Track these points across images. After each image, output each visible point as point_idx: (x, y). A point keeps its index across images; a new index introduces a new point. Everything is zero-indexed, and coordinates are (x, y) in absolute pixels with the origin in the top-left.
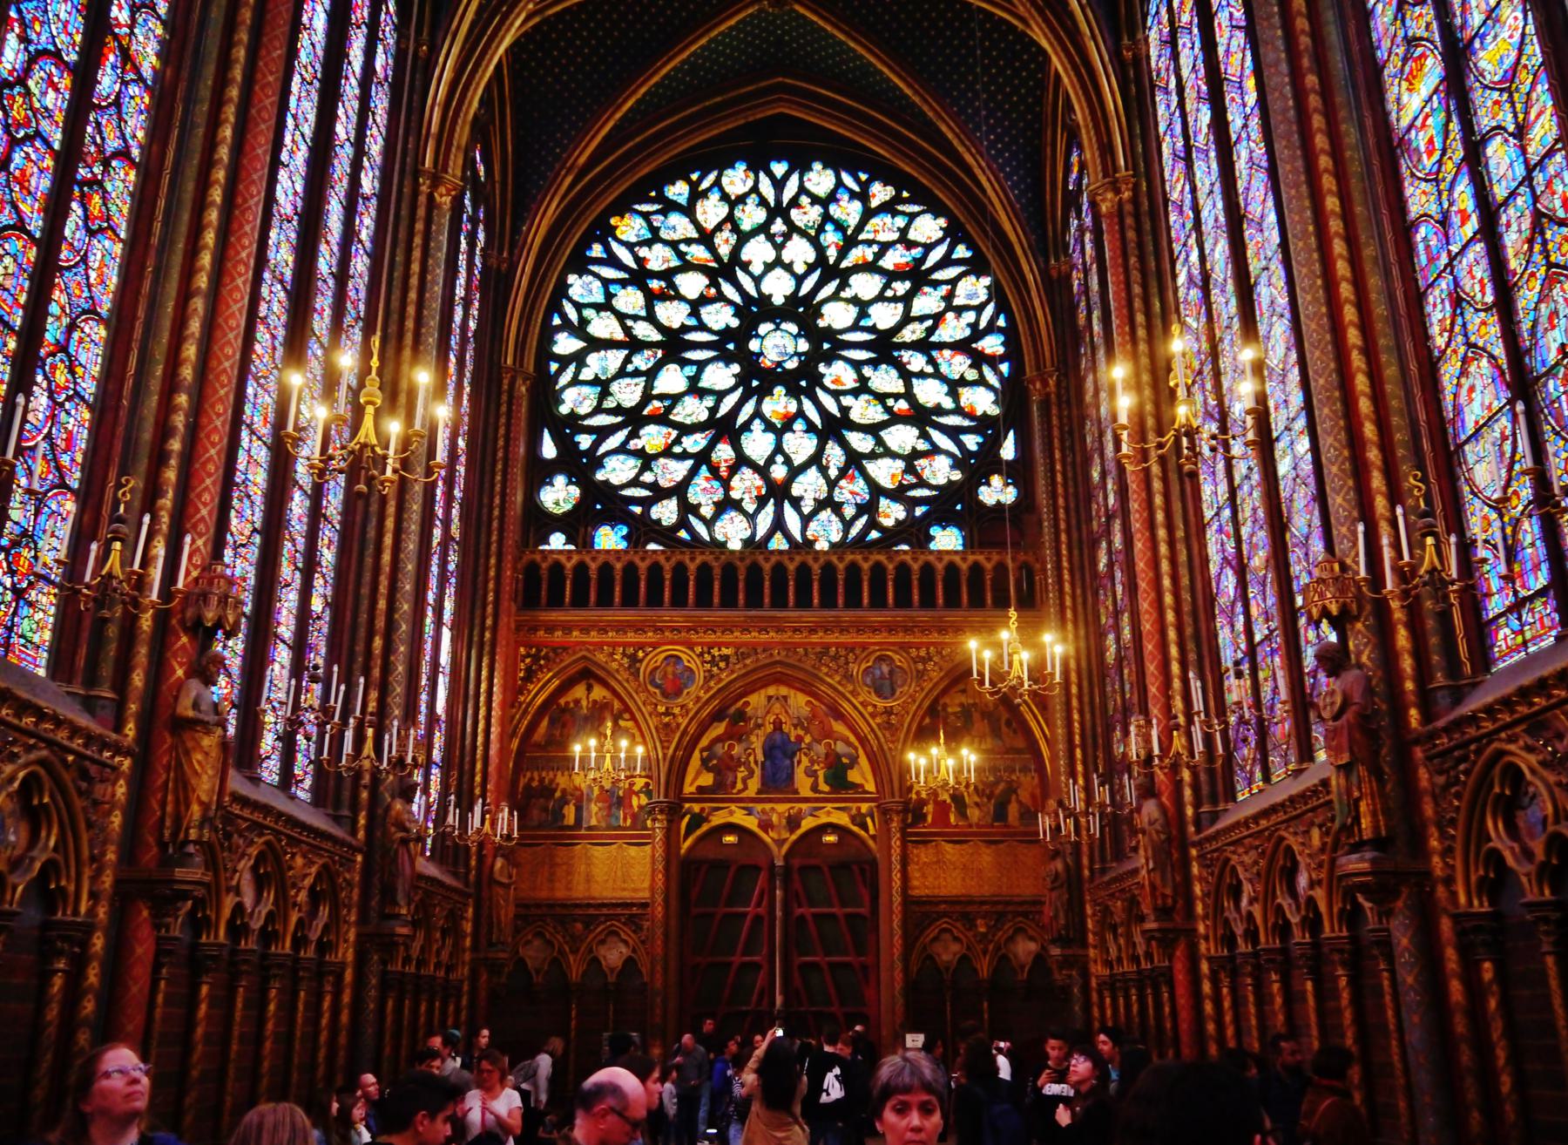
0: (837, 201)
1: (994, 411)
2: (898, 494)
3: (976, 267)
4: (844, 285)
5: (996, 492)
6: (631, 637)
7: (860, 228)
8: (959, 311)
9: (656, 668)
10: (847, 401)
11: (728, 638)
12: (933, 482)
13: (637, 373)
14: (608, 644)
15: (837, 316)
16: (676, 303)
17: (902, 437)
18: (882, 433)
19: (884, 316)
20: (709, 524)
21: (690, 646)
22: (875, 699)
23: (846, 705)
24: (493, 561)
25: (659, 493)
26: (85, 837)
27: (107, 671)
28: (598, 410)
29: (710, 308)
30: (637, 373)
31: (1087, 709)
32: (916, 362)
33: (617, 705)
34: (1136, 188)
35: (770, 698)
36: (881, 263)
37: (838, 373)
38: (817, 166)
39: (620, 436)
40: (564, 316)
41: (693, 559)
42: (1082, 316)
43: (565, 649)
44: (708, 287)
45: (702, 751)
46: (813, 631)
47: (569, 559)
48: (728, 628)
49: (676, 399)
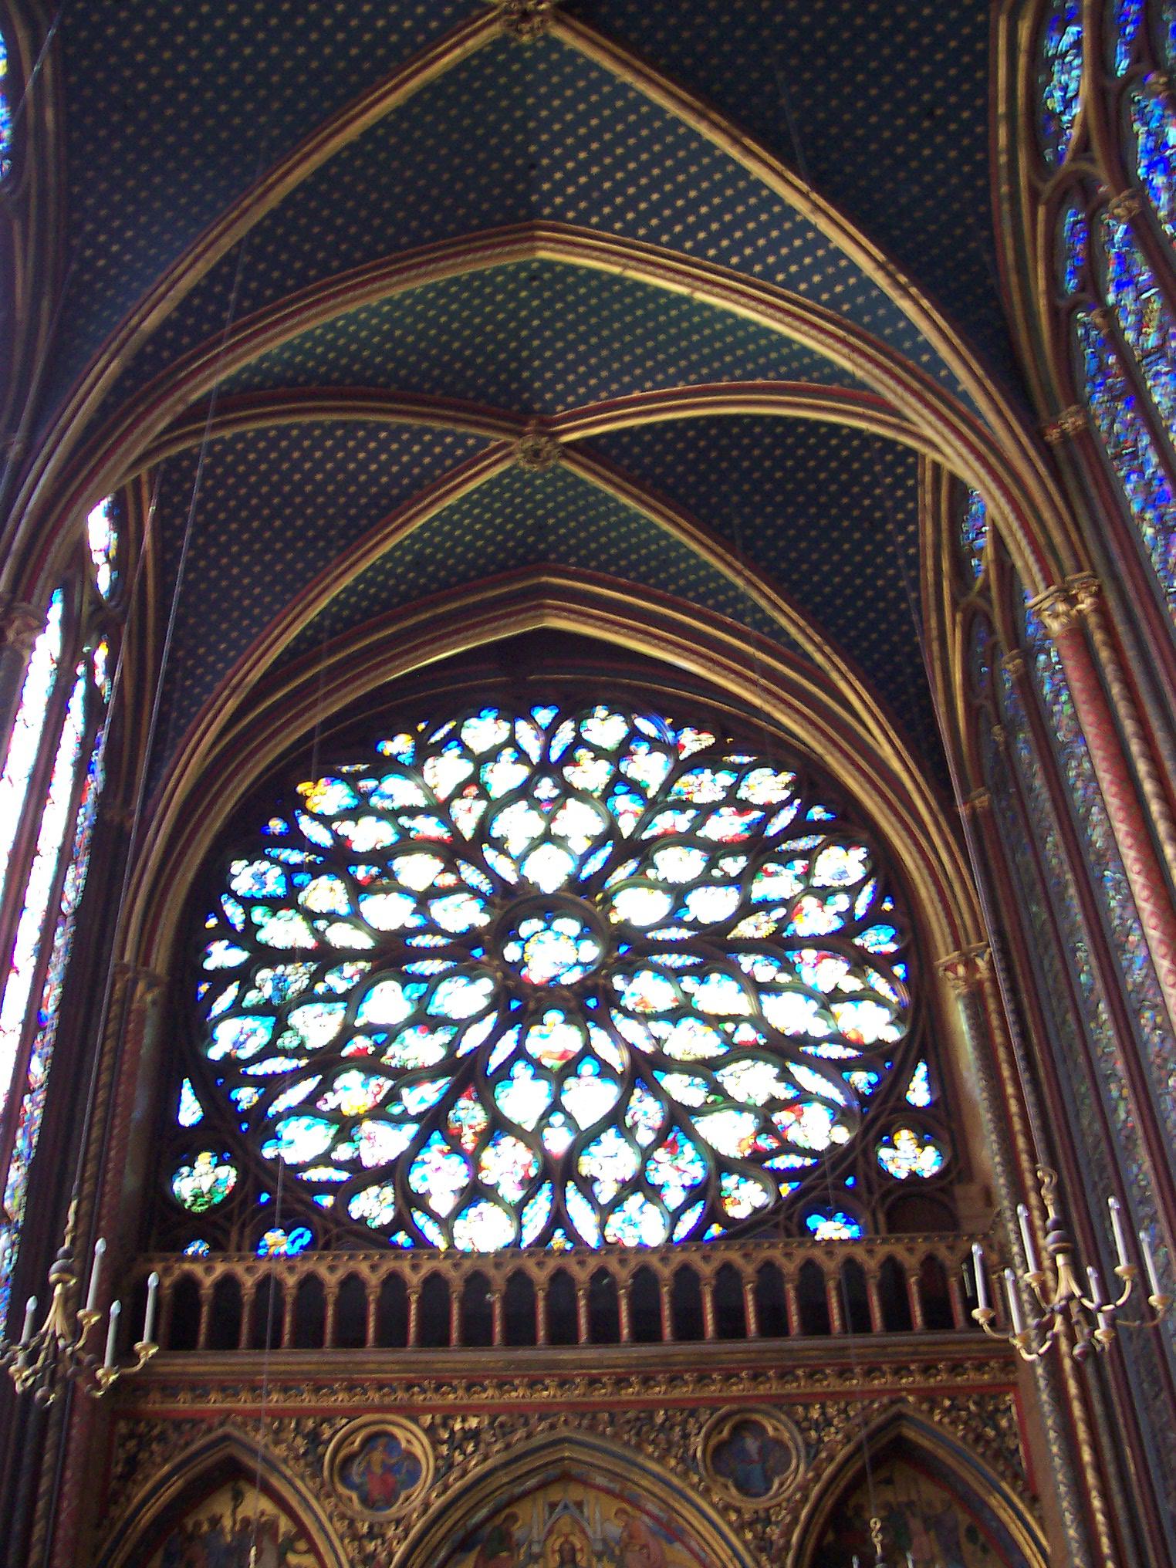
1: (892, 1035)
2: (753, 1165)
4: (647, 862)
7: (666, 787)
10: (660, 1028)
15: (638, 907)
16: (394, 895)
19: (712, 906)
21: (413, 1414)
28: (269, 1051)
30: (330, 997)
31: (1114, 1485)
32: (764, 970)
33: (284, 1525)
34: (1099, 595)
37: (647, 990)
38: (601, 711)
41: (415, 1267)
43: (195, 1421)
46: (621, 1382)
47: (209, 1270)
49: (392, 1033)
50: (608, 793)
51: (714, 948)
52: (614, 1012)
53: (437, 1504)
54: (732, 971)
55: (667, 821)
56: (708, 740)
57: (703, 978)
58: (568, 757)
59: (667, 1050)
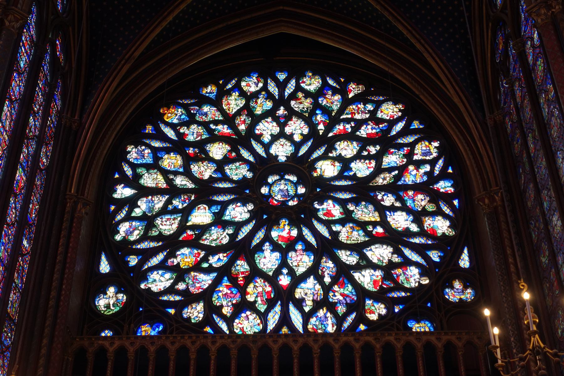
0: (324, 95)
2: (379, 296)
3: (426, 135)
4: (331, 148)
5: (457, 293)
7: (342, 110)
8: (418, 164)
12: (407, 285)
13: (175, 211)
17: (380, 253)
18: (365, 251)
19: (362, 169)
20: (230, 321)
24: (45, 341)
25: (189, 298)
29: (233, 166)
32: (389, 200)
36: (358, 133)
39: (161, 257)
42: (517, 146)
44: (230, 152)
47: (112, 344)
49: (204, 229)
51: (363, 190)
56: (361, 88)
57: (357, 205)
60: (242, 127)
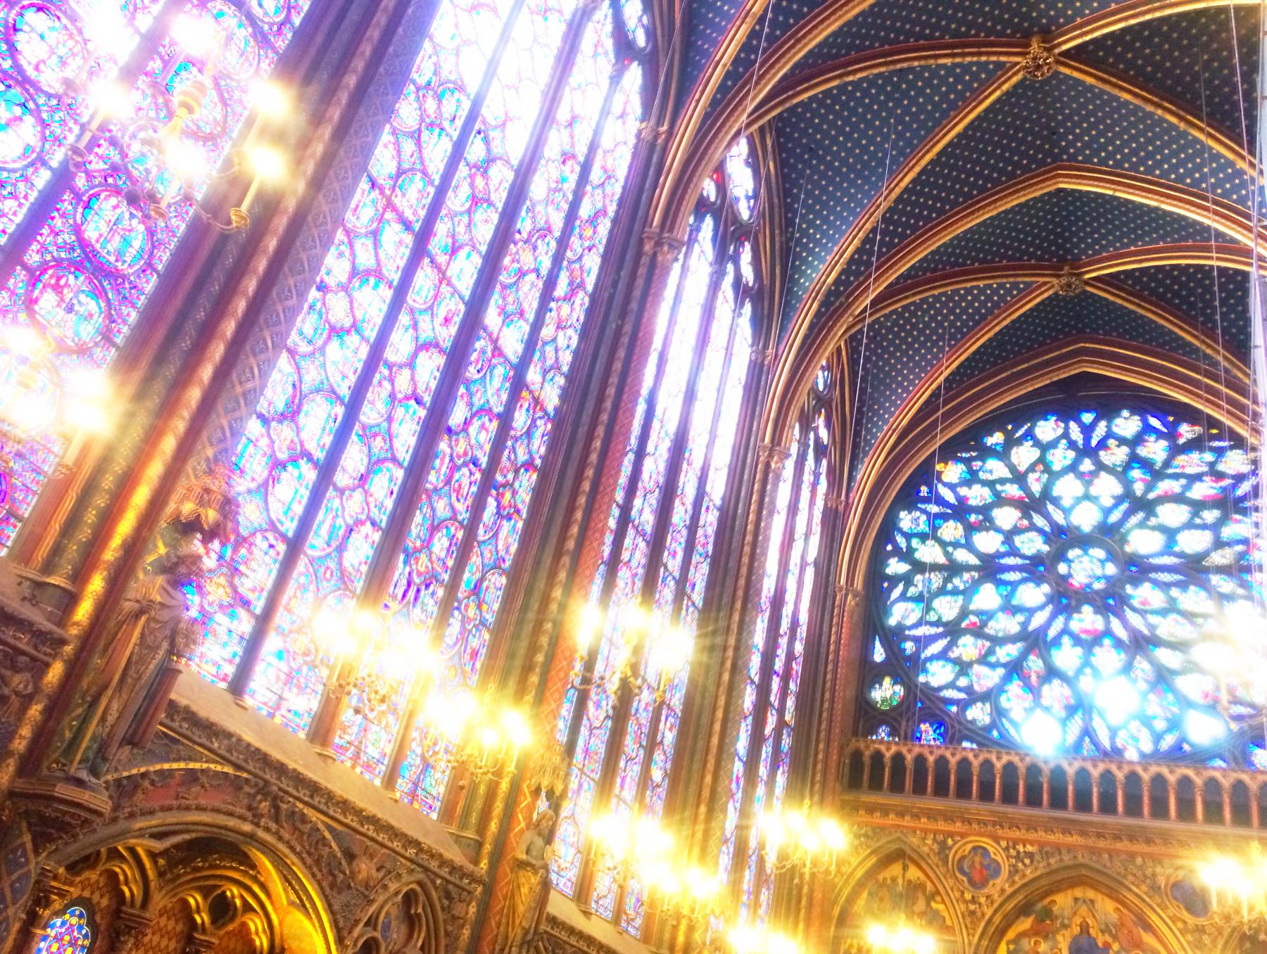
6: (942, 825)
7: (1167, 463)
9: (963, 858)
10: (1152, 619)
11: (1032, 836)
14: (922, 830)
15: (1143, 542)
16: (992, 533)
19: (1194, 542)
21: (997, 840)
22: (1186, 915)
23: (1154, 917)
25: (973, 697)
26: (443, 942)
27: (474, 818)
30: (955, 592)
33: (929, 885)
35: (1076, 900)
36: (1188, 494)
38: (1125, 413)
40: (896, 545)
41: (999, 758)
45: (1008, 943)
46: (1117, 838)
48: (1031, 826)
49: (987, 616)
50: (1127, 466)
52: (1127, 610)
53: (1009, 890)
54: (1204, 585)
55: (1165, 486)
58: (1102, 444)
59: (1158, 632)
60: (1036, 488)
